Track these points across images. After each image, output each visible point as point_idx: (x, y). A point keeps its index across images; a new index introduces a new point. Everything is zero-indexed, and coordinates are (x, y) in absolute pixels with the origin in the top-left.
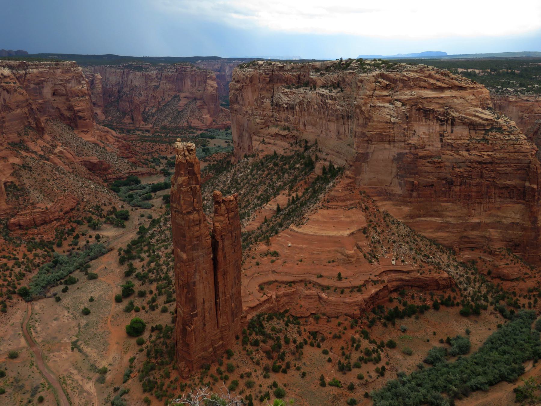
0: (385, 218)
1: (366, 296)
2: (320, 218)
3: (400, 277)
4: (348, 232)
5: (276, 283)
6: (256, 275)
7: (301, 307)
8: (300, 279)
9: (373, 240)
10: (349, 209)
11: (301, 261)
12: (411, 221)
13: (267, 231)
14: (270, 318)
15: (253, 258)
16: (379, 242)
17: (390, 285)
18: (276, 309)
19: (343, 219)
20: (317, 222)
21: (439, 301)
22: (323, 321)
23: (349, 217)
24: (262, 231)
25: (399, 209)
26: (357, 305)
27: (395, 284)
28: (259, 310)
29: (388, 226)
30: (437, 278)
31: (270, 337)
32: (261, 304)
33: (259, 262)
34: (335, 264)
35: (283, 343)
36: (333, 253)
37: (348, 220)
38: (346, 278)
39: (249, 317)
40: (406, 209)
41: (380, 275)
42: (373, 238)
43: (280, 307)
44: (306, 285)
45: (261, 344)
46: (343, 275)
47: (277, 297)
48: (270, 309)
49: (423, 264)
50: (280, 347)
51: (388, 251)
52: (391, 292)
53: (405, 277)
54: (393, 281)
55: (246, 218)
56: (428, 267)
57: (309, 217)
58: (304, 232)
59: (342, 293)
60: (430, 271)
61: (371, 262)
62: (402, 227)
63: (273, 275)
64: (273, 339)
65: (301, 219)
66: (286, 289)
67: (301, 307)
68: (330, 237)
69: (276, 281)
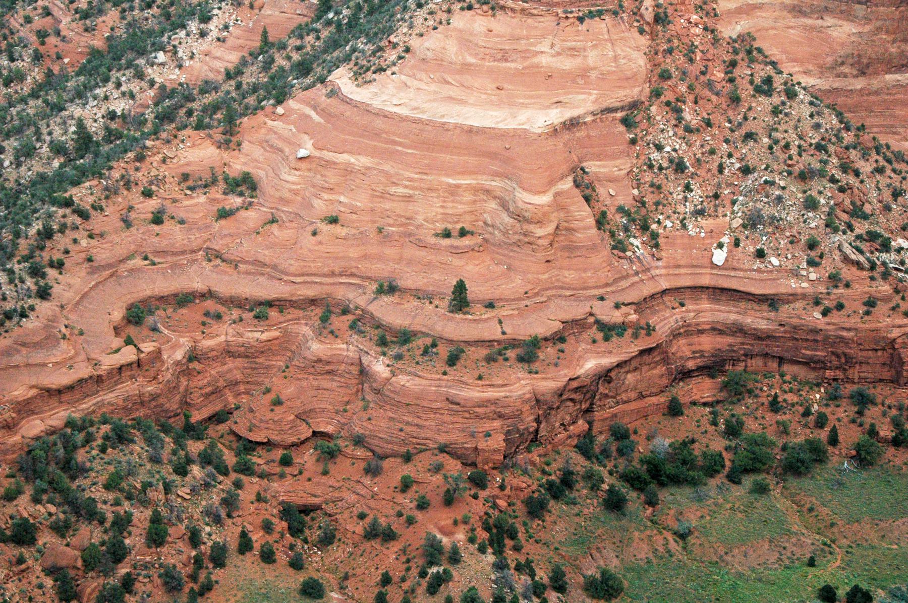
0: (733, 64)
1: (548, 383)
2: (452, 50)
3: (733, 317)
4: (556, 116)
5: (210, 305)
6: (138, 262)
7: (278, 402)
8: (310, 292)
9: (655, 155)
10: (581, 20)
11: (334, 221)
12: (859, 84)
13: (255, 89)
14: (120, 437)
15: (148, 194)
16: (680, 167)
17: (682, 348)
18: (173, 405)
19: (544, 60)
20: (436, 65)
21: (886, 431)
22: (343, 468)
23: (573, 52)
24: (239, 86)
25: (812, 28)
26: (501, 416)
27: (707, 343)
28: (87, 405)
29: (735, 100)
30: (895, 333)
31: (90, 513)
32: (99, 380)
33: (171, 209)
34: (466, 241)
35: (134, 540)
36: (468, 197)
37: (567, 64)
38: (491, 305)
39: (34, 427)
40: (843, 31)
41: (642, 305)
42: (659, 148)
43: (196, 398)
44: (324, 319)
45: (46, 538)
46: (474, 291)
47: (193, 356)
48: (142, 403)
49: (847, 273)
50: (118, 554)
51: (709, 206)
52: (685, 375)
53: (758, 320)
54: (701, 332)
55: (194, 26)
56: (863, 286)
57: (414, 42)
58: (377, 103)
59: (452, 360)
60: (871, 303)
61: (620, 247)
62: (801, 109)
63: (208, 266)
64: (102, 522)
65: (380, 49)
66: (239, 328)
67: (278, 402)
68: (470, 130)
69: (209, 294)
